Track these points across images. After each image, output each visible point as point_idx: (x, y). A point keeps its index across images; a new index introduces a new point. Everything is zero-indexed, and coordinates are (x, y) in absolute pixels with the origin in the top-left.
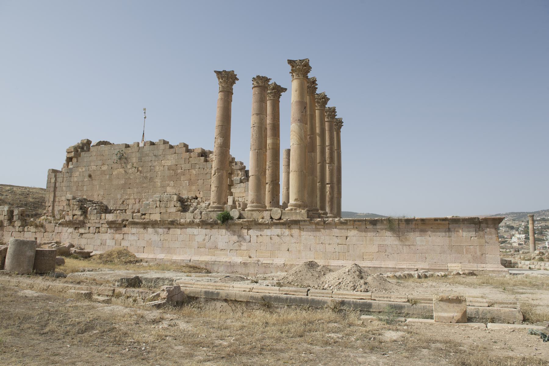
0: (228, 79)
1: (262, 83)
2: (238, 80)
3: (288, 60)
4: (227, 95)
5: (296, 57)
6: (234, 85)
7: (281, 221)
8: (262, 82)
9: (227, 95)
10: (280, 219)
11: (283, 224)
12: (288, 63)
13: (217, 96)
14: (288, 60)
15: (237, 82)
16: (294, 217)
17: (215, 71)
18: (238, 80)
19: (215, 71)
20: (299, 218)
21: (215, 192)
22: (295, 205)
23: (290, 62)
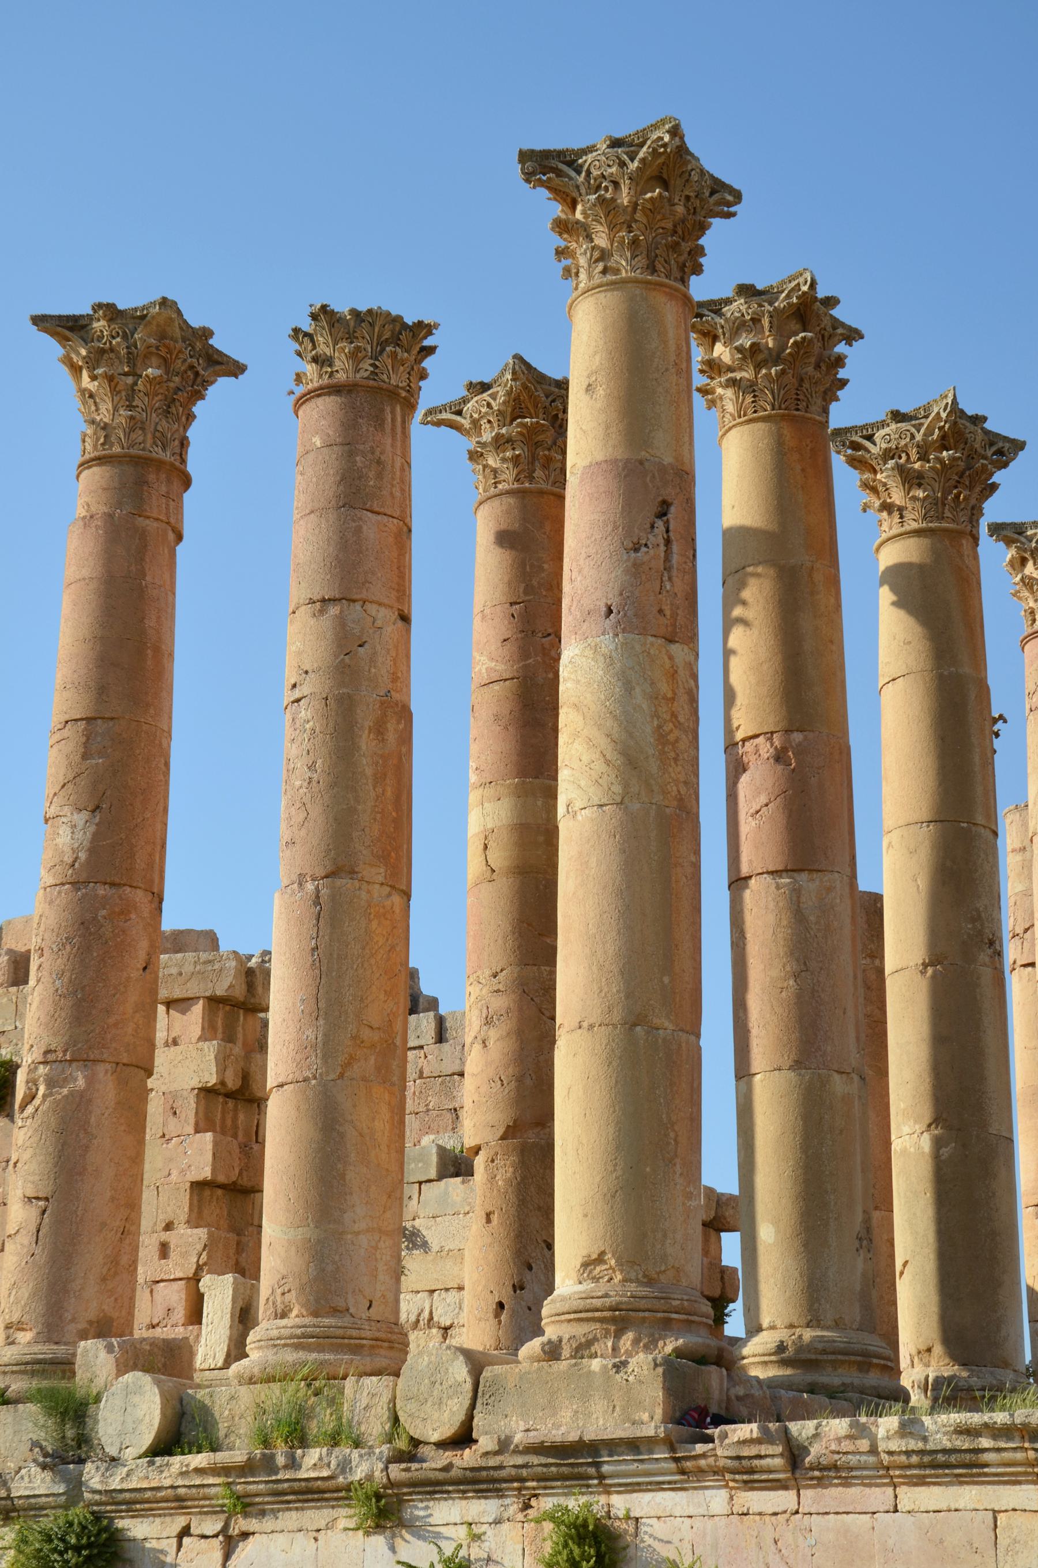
0: (150, 371)
1: (372, 364)
2: (236, 369)
3: (525, 156)
4: (143, 481)
5: (580, 128)
6: (200, 403)
7: (468, 1457)
8: (355, 356)
9: (143, 481)
10: (463, 1438)
11: (480, 1483)
12: (528, 177)
13: (66, 503)
14: (525, 156)
15: (221, 389)
16: (566, 1415)
17: (40, 321)
18: (236, 369)
19: (40, 321)
20: (600, 1423)
21: (25, 1239)
22: (581, 1314)
23: (547, 167)
